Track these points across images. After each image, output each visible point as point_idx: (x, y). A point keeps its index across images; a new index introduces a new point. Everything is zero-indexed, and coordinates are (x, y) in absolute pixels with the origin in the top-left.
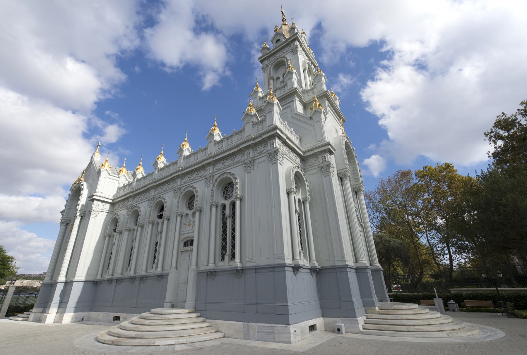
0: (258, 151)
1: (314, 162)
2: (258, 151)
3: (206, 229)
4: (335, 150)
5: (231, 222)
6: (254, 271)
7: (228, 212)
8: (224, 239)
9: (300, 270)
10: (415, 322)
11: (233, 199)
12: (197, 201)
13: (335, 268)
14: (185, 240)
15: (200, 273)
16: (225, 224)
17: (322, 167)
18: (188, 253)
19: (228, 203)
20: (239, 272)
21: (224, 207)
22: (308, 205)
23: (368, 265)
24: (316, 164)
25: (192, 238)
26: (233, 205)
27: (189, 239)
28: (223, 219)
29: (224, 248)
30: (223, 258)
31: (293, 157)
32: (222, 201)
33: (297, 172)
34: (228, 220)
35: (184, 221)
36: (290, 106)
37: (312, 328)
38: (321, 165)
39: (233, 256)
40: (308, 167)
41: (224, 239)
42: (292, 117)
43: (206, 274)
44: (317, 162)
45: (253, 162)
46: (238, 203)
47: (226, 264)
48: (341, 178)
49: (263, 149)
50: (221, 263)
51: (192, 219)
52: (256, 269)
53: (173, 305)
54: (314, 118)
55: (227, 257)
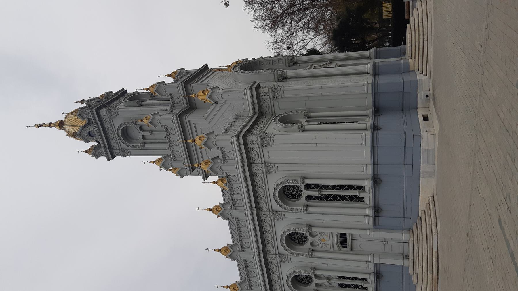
0: (256, 157)
1: (266, 104)
2: (256, 157)
3: (330, 219)
4: (255, 83)
5: (326, 190)
6: (376, 166)
7: (315, 193)
8: (343, 198)
9: (376, 125)
10: (421, 33)
11: (302, 187)
12: (299, 230)
13: (374, 93)
14: (340, 246)
15: (375, 225)
16: (327, 198)
17: (273, 97)
18: (355, 242)
19: (306, 193)
20: (376, 181)
21: (309, 198)
22: (312, 114)
23: (371, 62)
24: (269, 102)
25: (339, 235)
26: (308, 187)
27: (339, 241)
28: (322, 200)
29: (351, 198)
30: (361, 199)
31: (262, 124)
32: (303, 200)
33: (279, 121)
34: (323, 193)
35: (319, 248)
36: (195, 124)
37: (425, 118)
38: (271, 97)
39: (360, 188)
40: (270, 110)
41: (343, 198)
42: (209, 123)
43: (377, 218)
44: (267, 101)
45: (267, 164)
46: (309, 182)
47: (368, 195)
48: (283, 79)
49: (255, 153)
50: (367, 200)
51: (318, 237)
52: (374, 164)
53: (406, 256)
54: (217, 100)
55: (362, 195)
